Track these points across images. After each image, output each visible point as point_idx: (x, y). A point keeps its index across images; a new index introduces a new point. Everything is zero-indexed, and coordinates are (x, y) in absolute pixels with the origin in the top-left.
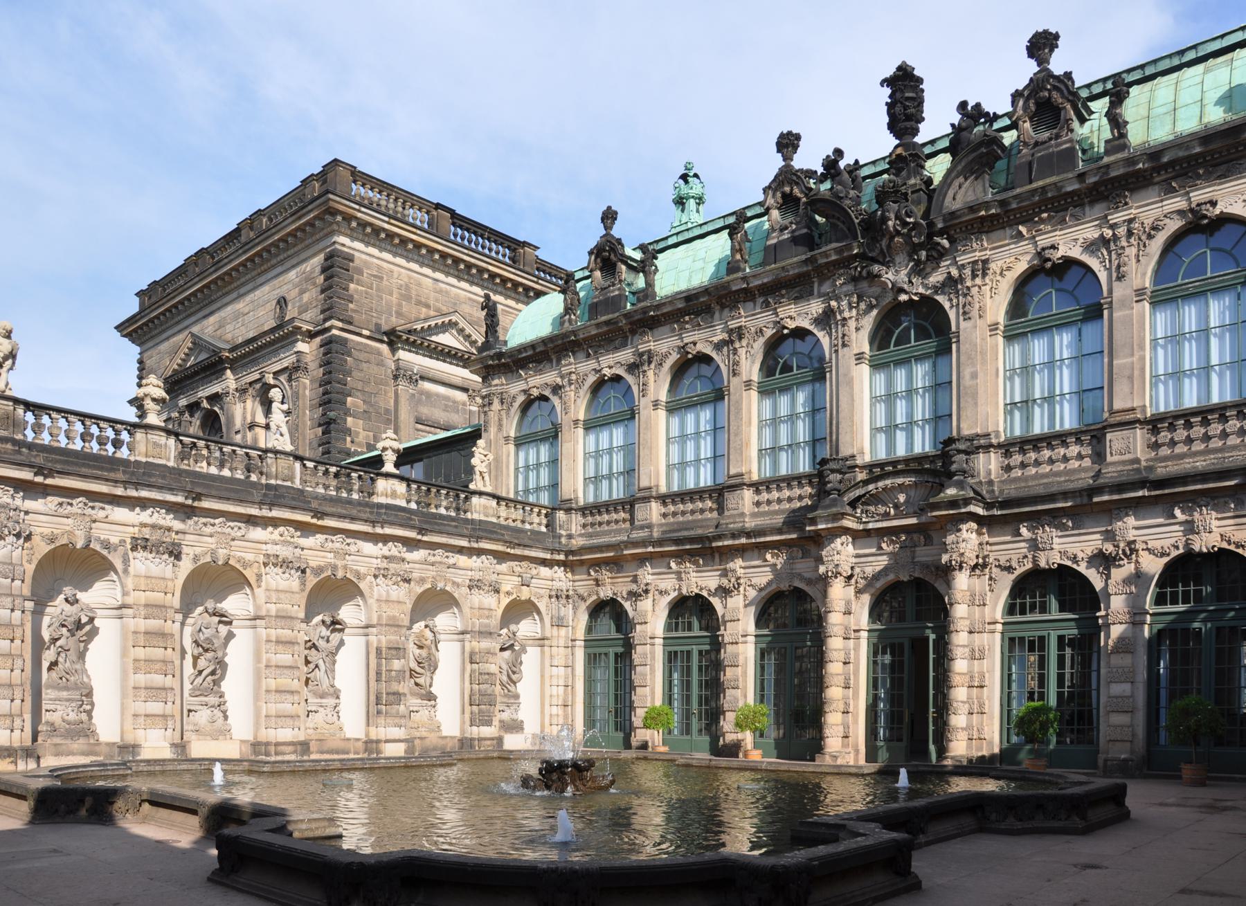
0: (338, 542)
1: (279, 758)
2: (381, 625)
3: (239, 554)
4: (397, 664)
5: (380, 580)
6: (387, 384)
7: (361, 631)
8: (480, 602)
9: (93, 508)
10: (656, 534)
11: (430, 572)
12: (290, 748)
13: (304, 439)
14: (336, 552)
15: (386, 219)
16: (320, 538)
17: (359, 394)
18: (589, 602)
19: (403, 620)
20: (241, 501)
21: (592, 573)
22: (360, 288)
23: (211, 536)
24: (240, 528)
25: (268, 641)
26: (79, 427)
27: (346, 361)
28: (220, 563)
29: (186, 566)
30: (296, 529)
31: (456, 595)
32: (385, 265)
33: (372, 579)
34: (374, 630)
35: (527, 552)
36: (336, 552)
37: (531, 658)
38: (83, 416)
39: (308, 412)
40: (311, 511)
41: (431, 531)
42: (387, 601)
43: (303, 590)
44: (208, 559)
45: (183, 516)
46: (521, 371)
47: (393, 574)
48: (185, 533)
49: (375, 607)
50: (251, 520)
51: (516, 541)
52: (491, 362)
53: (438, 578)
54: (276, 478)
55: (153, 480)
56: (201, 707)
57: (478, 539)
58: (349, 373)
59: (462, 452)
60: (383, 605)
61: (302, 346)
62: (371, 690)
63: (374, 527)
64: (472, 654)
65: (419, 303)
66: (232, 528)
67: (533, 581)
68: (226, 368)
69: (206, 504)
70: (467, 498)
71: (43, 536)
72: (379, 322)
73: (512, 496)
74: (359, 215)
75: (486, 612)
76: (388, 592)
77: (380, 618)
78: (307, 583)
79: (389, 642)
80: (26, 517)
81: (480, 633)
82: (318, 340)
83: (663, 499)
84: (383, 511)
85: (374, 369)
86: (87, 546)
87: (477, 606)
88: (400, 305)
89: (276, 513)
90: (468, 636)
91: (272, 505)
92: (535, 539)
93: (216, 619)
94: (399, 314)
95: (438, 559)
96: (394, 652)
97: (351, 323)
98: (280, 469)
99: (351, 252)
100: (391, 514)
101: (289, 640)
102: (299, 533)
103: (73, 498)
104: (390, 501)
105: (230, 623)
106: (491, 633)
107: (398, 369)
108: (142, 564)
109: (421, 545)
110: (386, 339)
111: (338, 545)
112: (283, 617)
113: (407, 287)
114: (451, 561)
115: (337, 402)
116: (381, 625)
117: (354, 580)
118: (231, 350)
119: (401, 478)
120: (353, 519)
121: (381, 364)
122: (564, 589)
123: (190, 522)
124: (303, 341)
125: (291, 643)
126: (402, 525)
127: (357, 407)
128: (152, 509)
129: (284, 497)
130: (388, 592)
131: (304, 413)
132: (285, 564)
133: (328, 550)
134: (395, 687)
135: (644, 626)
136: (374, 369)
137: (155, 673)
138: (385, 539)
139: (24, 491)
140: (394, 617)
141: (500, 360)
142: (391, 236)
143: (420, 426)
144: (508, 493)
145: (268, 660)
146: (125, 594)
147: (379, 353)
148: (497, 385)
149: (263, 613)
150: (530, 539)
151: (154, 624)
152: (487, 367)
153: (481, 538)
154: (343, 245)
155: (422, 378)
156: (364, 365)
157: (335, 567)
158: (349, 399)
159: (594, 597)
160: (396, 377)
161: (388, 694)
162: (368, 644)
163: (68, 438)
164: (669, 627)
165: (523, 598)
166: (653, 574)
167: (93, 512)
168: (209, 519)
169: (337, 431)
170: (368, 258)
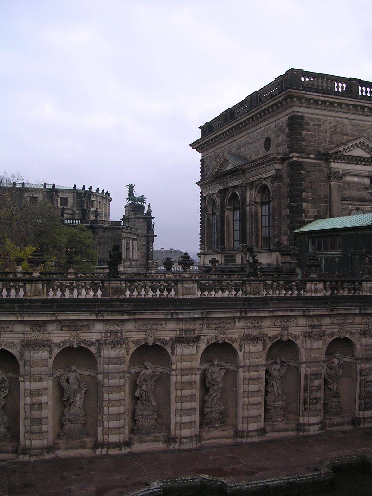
3: (230, 336)
4: (316, 383)
11: (336, 329)
15: (321, 95)
19: (320, 358)
22: (308, 133)
27: (301, 173)
29: (203, 346)
32: (322, 117)
43: (264, 350)
44: (214, 341)
65: (342, 134)
72: (320, 149)
74: (306, 96)
78: (267, 346)
88: (331, 137)
94: (331, 142)
96: (315, 376)
98: (252, 289)
99: (303, 115)
101: (256, 377)
113: (335, 127)
117: (293, 340)
125: (258, 379)
127: (308, 197)
134: (315, 395)
137: (186, 402)
140: (315, 357)
142: (324, 102)
143: (344, 202)
151: (186, 378)
154: (298, 112)
155: (345, 175)
156: (312, 174)
170: (312, 116)
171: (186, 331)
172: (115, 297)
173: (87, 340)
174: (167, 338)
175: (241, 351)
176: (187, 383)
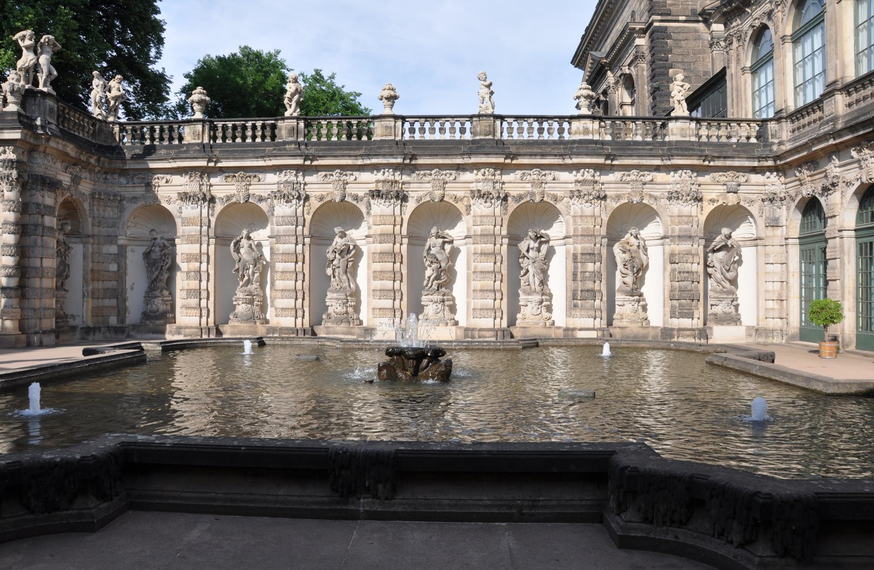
0: (534, 175)
1: (481, 340)
2: (577, 236)
3: (452, 193)
4: (590, 267)
5: (575, 201)
6: (704, 52)
7: (563, 242)
8: (679, 211)
9: (346, 175)
10: (839, 126)
11: (627, 189)
12: (491, 333)
13: (644, 108)
14: (533, 183)
16: (519, 173)
17: (679, 65)
18: (797, 201)
20: (447, 155)
21: (797, 174)
23: (429, 182)
24: (451, 174)
25: (475, 254)
26: (536, 125)
28: (436, 200)
29: (411, 205)
30: (692, 171)
31: (654, 206)
33: (568, 199)
34: (571, 240)
35: (729, 163)
36: (533, 183)
37: (748, 254)
38: (427, 118)
39: (646, 87)
40: (503, 154)
41: (620, 156)
42: (581, 216)
44: (428, 198)
45: (409, 172)
46: (747, 9)
47: (585, 195)
48: (409, 183)
49: (571, 220)
50: (460, 168)
51: (716, 155)
52: (725, 9)
53: (633, 194)
54: (480, 135)
55: (485, 150)
56: (429, 303)
57: (670, 156)
58: (670, 51)
59: (720, 90)
60: (579, 220)
61: (639, 41)
62: (568, 288)
63: (564, 159)
64: (672, 255)
66: (446, 175)
67: (741, 187)
68: (606, 71)
69: (421, 161)
70: (664, 126)
71: (315, 197)
73: (750, 117)
75: (685, 219)
76: (582, 208)
77: (575, 230)
78: (509, 208)
79: (582, 248)
80: (603, 187)
81: (679, 237)
82: (647, 35)
83: (847, 89)
84: (575, 145)
85: (692, 44)
86: (343, 200)
87: (676, 213)
89: (474, 160)
90: (668, 240)
91: (470, 154)
92: (744, 149)
93: (441, 240)
95: (633, 177)
96: (588, 257)
97: (669, 15)
100: (683, 148)
102: (695, 174)
103: (333, 171)
104: (582, 137)
105: (451, 242)
106: (690, 237)
107: (712, 38)
108: (380, 207)
109: (615, 168)
110: (700, 19)
111: (535, 177)
112: (486, 235)
114: (648, 178)
115: (660, 74)
116: (577, 236)
117: (552, 202)
118: (607, 57)
119: (691, 119)
120: (543, 155)
121: (698, 39)
122: (778, 192)
123: (414, 175)
124: (640, 37)
126: (587, 155)
128: (583, 170)
129: (484, 147)
130: (582, 208)
131: (643, 88)
132: (483, 196)
133: (526, 181)
134: (589, 285)
135: (834, 219)
136: (692, 44)
138: (577, 167)
139: (697, 172)
141: (731, 5)
144: (746, 115)
145: (475, 268)
146: (369, 228)
147: (696, 31)
148: (734, 27)
149: (472, 233)
150: (734, 151)
152: (725, 14)
153: (672, 156)
156: (683, 42)
157: (533, 194)
158: (671, 71)
159: (800, 197)
160: (711, 46)
161: (582, 291)
162: (567, 252)
163: (549, 133)
164: (860, 218)
165: (730, 204)
166: (840, 167)
167: (347, 178)
168: (426, 171)
169: (661, 96)
171: (384, 182)
172: (291, 139)
173: (257, 194)
174: (361, 194)
175: (468, 214)
176: (386, 253)
